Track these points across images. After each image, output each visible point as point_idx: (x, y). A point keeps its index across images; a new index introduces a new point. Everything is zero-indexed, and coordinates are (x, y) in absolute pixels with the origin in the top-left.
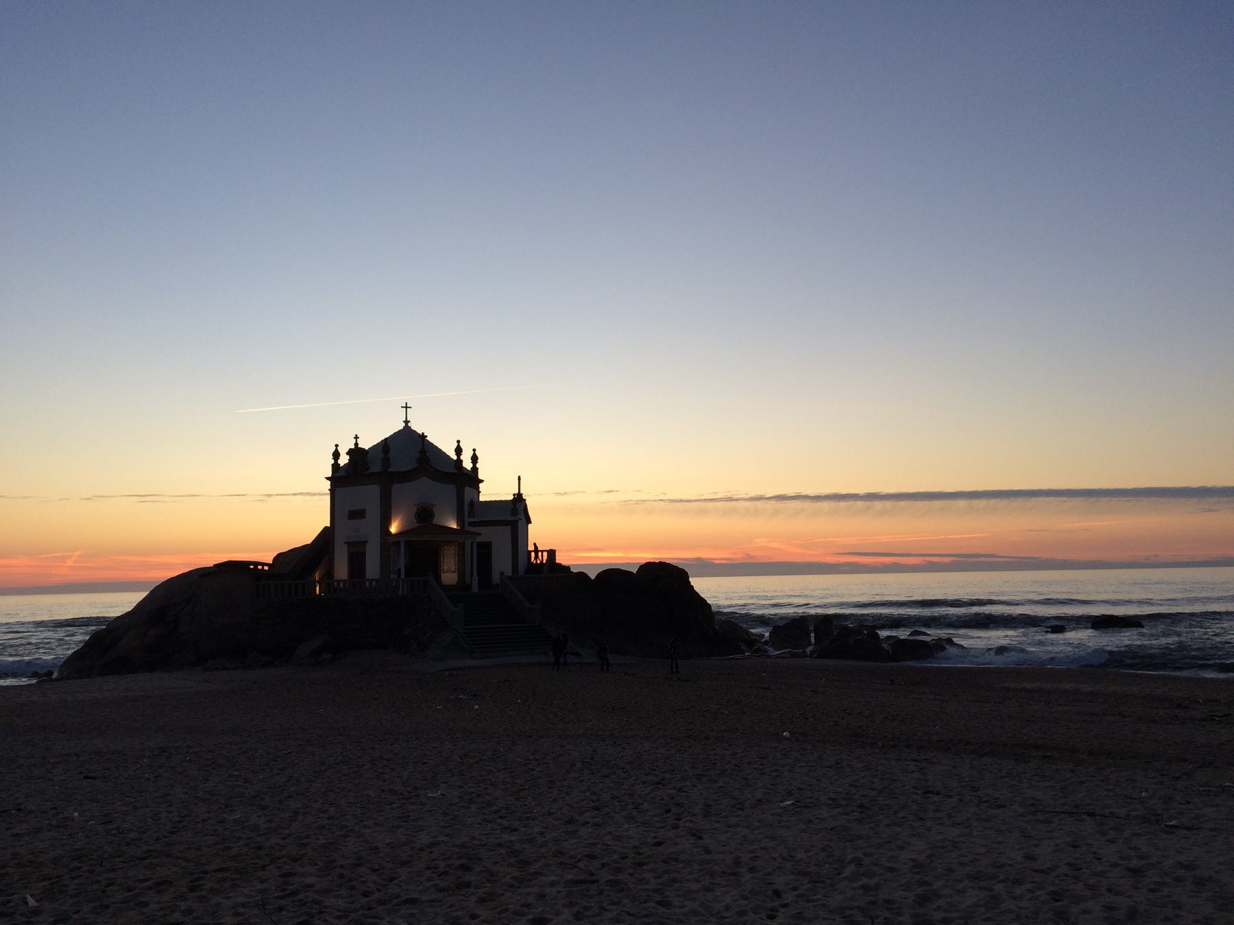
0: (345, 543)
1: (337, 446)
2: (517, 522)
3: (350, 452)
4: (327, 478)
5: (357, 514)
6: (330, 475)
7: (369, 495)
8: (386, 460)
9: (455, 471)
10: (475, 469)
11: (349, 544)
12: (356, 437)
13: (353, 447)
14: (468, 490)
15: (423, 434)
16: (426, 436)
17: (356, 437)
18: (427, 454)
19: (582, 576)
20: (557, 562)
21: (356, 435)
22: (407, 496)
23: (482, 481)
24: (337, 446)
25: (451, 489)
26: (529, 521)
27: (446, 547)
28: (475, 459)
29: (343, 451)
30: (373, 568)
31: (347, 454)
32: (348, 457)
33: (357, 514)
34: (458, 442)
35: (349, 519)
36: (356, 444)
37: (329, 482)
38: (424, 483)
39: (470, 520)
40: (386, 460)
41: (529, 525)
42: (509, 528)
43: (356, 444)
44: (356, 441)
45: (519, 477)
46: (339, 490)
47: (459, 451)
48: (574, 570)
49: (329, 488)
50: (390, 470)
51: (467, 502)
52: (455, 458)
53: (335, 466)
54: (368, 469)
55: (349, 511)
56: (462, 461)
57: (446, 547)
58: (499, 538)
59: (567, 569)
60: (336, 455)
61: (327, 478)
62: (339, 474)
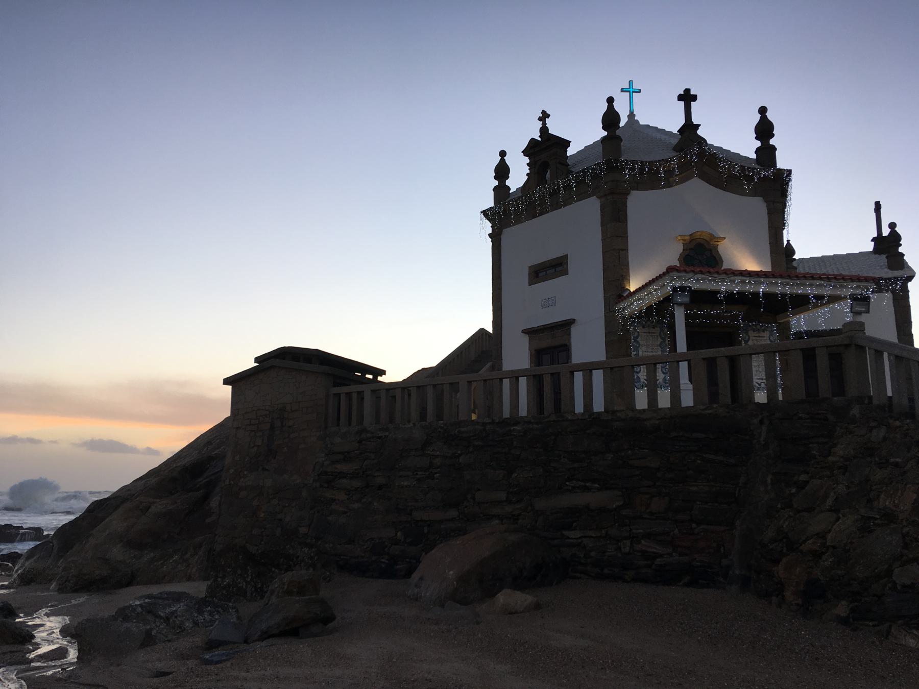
0: (525, 332)
1: (503, 154)
3: (532, 150)
4: (485, 213)
11: (531, 332)
12: (545, 116)
15: (687, 91)
16: (694, 98)
17: (545, 116)
18: (699, 132)
21: (544, 112)
24: (503, 154)
25: (757, 206)
27: (751, 333)
31: (526, 152)
32: (527, 160)
34: (763, 111)
35: (530, 285)
36: (544, 130)
38: (696, 188)
45: (878, 206)
46: (508, 234)
47: (764, 130)
53: (501, 191)
55: (530, 267)
56: (774, 149)
57: (751, 333)
60: (502, 171)
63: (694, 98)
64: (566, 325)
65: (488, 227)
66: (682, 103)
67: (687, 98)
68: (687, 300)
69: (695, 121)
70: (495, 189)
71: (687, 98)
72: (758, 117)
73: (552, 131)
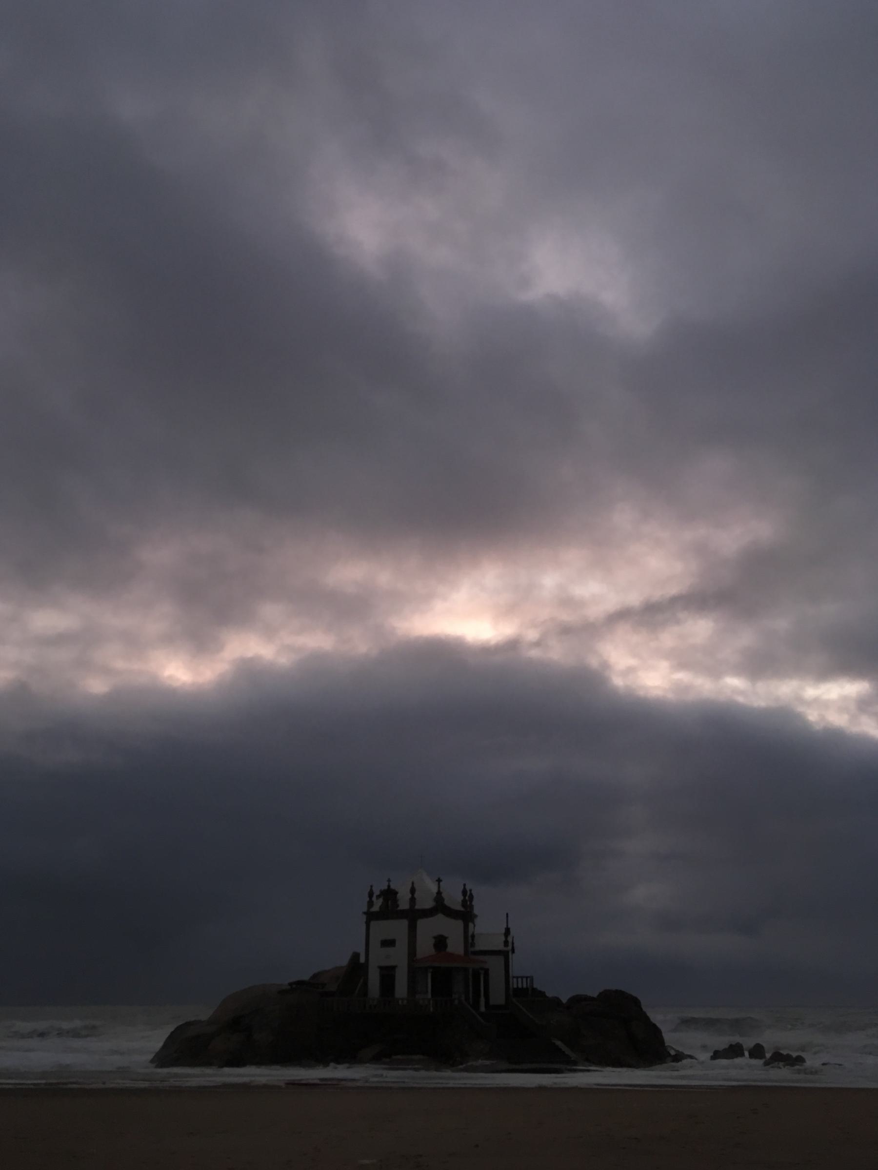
1: (371, 886)
2: (508, 952)
4: (364, 913)
5: (388, 943)
6: (365, 909)
7: (398, 929)
8: (413, 900)
9: (462, 909)
10: (472, 907)
11: (382, 968)
12: (389, 881)
13: (386, 888)
14: (471, 925)
15: (439, 879)
16: (441, 881)
17: (389, 881)
18: (443, 895)
19: (557, 1001)
20: (535, 986)
22: (428, 929)
23: (476, 916)
25: (459, 924)
26: (513, 952)
28: (471, 897)
29: (377, 892)
30: (401, 989)
33: (388, 943)
35: (381, 947)
36: (389, 886)
37: (365, 917)
38: (440, 917)
39: (472, 949)
40: (413, 900)
41: (513, 955)
42: (501, 959)
43: (389, 886)
44: (389, 884)
45: (507, 914)
47: (464, 892)
48: (550, 994)
49: (365, 920)
50: (417, 907)
51: (470, 933)
52: (462, 898)
53: (371, 904)
54: (398, 906)
58: (495, 965)
59: (542, 994)
60: (371, 894)
61: (364, 913)
62: (376, 908)
63: (441, 881)
64: (393, 968)
65: (364, 918)
66: (437, 883)
67: (439, 881)
68: (431, 970)
69: (441, 890)
70: (369, 902)
71: (439, 881)
72: (463, 887)
73: (392, 887)
